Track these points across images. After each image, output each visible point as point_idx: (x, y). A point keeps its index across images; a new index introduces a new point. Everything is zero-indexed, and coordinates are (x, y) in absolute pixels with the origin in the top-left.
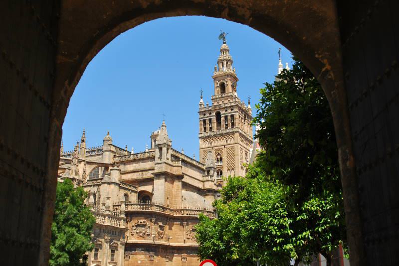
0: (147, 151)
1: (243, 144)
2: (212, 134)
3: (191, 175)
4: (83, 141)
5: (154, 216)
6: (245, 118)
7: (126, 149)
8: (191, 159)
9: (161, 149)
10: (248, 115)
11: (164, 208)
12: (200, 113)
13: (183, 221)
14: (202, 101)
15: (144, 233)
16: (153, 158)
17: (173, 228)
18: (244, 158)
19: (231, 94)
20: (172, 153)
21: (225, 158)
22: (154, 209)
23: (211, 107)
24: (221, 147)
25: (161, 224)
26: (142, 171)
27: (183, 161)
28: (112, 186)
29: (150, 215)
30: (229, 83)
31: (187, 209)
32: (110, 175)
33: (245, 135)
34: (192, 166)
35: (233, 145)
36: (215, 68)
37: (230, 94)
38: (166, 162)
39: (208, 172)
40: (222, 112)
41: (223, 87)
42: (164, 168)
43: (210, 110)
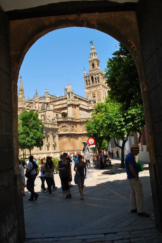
0: (63, 95)
2: (90, 86)
4: (37, 94)
6: (104, 78)
7: (54, 96)
9: (69, 94)
11: (73, 119)
12: (84, 77)
13: (81, 123)
14: (85, 72)
15: (66, 130)
17: (77, 126)
21: (96, 96)
22: (69, 120)
25: (72, 125)
26: (62, 104)
27: (79, 98)
28: (51, 111)
29: (67, 122)
30: (96, 63)
39: (90, 102)
40: (94, 76)
41: (93, 65)
42: (71, 102)
43: (89, 76)
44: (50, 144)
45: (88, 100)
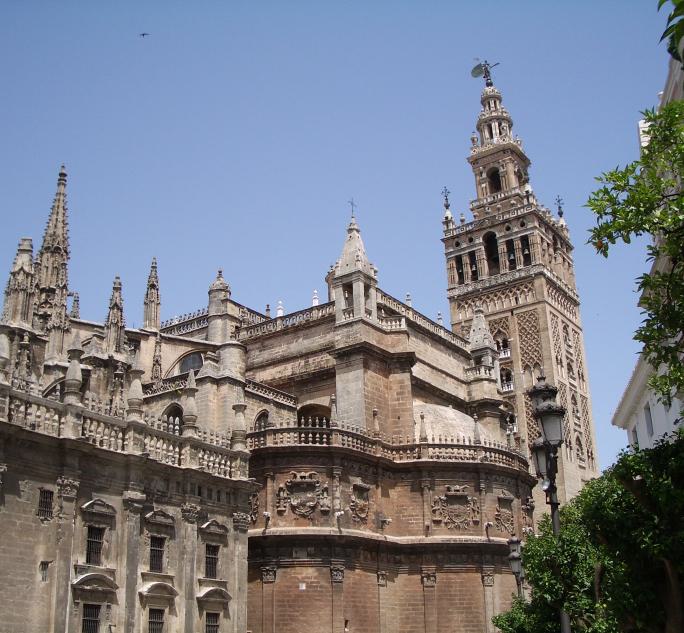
1: (556, 305)
2: (479, 286)
3: (434, 365)
4: (153, 286)
5: (338, 461)
6: (555, 244)
8: (433, 323)
10: (561, 238)
11: (364, 440)
14: (449, 214)
15: (313, 508)
16: (332, 318)
18: (562, 340)
19: (517, 191)
20: (380, 301)
21: (515, 339)
22: (337, 442)
23: (471, 224)
24: (503, 315)
25: (358, 481)
27: (410, 323)
28: (225, 388)
30: (510, 169)
31: (430, 442)
32: (217, 362)
33: (559, 282)
34: (437, 341)
35: (534, 307)
36: (473, 140)
37: (513, 192)
38: (365, 319)
39: (478, 361)
41: (495, 181)
44: (173, 593)
45: (467, 342)
